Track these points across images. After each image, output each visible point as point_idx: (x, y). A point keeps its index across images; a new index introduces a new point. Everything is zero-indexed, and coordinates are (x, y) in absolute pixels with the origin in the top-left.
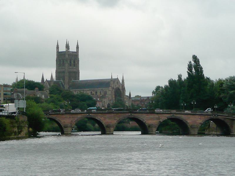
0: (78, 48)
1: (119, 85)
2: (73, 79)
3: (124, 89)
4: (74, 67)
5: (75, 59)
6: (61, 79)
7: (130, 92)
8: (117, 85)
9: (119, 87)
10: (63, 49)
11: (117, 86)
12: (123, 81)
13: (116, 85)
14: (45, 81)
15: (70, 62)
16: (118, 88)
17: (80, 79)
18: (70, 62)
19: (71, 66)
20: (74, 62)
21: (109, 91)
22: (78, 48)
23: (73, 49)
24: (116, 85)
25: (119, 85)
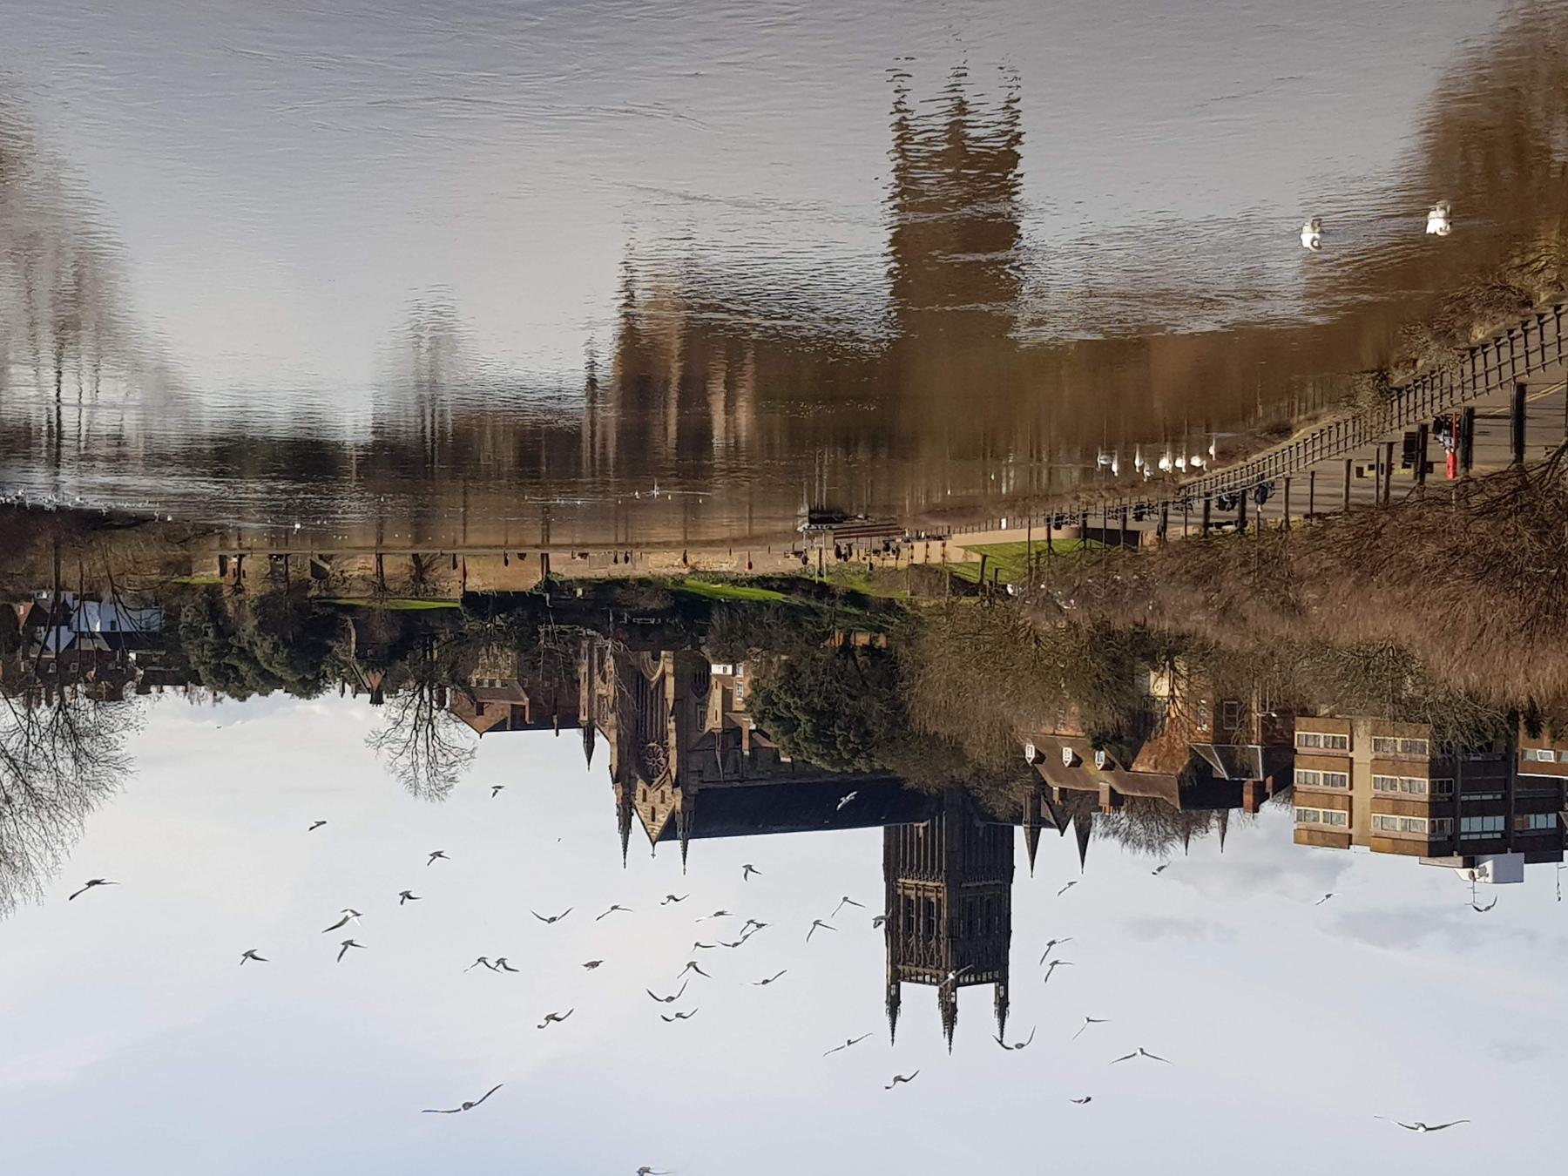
0: (894, 1004)
1: (645, 800)
2: (921, 831)
3: (621, 777)
4: (912, 894)
5: (906, 945)
6: (981, 834)
7: (589, 761)
8: (658, 800)
9: (645, 792)
10: (976, 999)
11: (654, 796)
12: (625, 827)
13: (663, 802)
14: (1071, 827)
15: (929, 925)
16: (650, 784)
17: (881, 829)
18: (929, 925)
19: (929, 903)
20: (909, 921)
21: (700, 772)
22: (894, 1004)
23: (920, 997)
24: (663, 802)
25: (645, 800)
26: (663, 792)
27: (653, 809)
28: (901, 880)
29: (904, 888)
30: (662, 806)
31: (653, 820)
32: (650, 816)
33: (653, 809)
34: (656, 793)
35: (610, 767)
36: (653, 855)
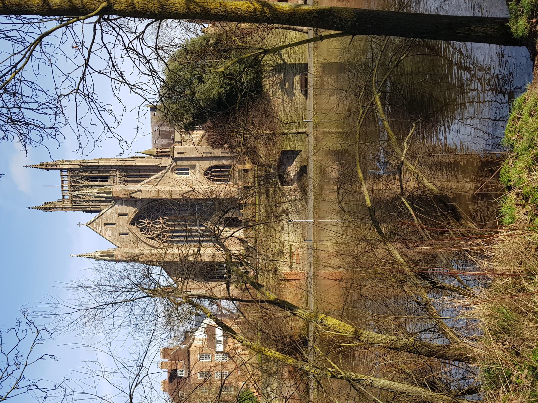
1: (120, 215)
13: (121, 234)
16: (133, 223)
24: (121, 234)
25: (120, 215)
26: (127, 234)
27: (114, 224)
28: (118, 173)
29: (114, 176)
30: (117, 234)
31: (106, 224)
32: (108, 222)
33: (114, 224)
34: (126, 228)
35: (141, 191)
36: (79, 225)
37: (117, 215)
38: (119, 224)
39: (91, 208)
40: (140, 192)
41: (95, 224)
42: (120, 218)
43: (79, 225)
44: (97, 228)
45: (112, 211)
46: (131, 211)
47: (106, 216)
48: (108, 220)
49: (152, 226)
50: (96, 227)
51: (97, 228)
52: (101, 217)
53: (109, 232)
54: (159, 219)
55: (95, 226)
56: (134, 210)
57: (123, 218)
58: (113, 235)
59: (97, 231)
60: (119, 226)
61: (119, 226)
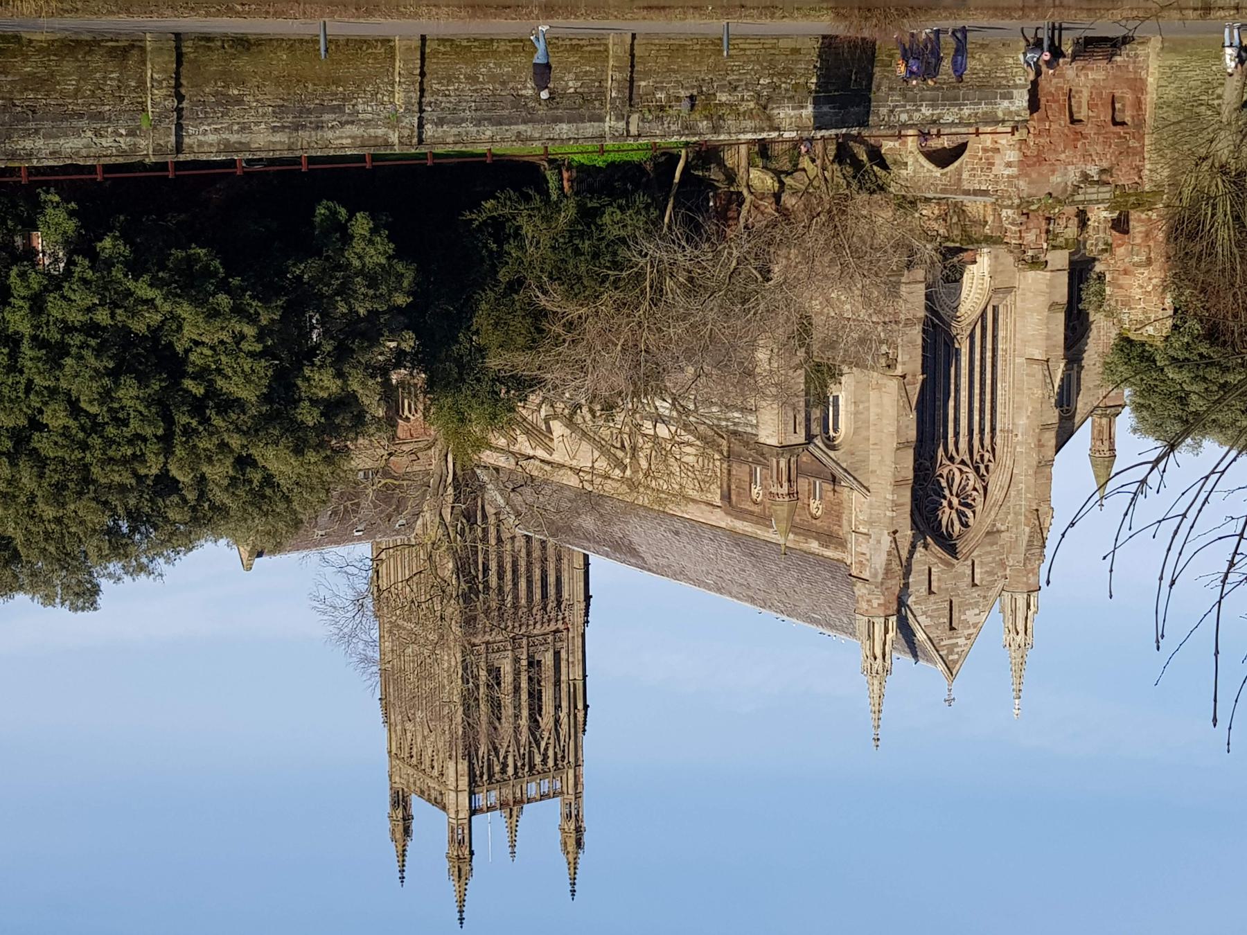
30: (975, 593)
37: (932, 597)
38: (953, 590)
39: (576, 707)
40: (897, 535)
41: (951, 657)
42: (939, 588)
43: (949, 701)
44: (959, 649)
45: (924, 613)
46: (928, 557)
47: (933, 629)
48: (942, 620)
49: (957, 496)
50: (957, 653)
51: (959, 649)
52: (935, 642)
53: (970, 615)
54: (941, 475)
55: (956, 657)
56: (921, 549)
57: (939, 580)
58: (977, 604)
59: (966, 649)
60: (958, 588)
61: (956, 588)
